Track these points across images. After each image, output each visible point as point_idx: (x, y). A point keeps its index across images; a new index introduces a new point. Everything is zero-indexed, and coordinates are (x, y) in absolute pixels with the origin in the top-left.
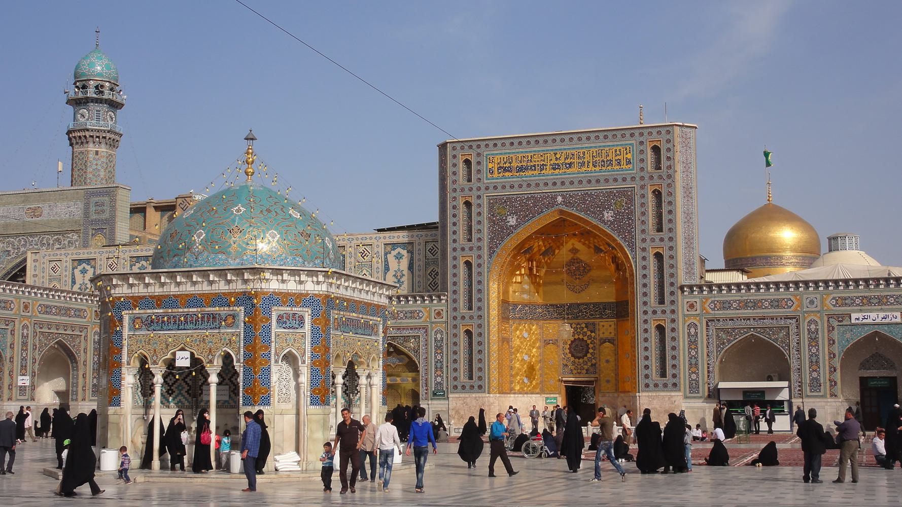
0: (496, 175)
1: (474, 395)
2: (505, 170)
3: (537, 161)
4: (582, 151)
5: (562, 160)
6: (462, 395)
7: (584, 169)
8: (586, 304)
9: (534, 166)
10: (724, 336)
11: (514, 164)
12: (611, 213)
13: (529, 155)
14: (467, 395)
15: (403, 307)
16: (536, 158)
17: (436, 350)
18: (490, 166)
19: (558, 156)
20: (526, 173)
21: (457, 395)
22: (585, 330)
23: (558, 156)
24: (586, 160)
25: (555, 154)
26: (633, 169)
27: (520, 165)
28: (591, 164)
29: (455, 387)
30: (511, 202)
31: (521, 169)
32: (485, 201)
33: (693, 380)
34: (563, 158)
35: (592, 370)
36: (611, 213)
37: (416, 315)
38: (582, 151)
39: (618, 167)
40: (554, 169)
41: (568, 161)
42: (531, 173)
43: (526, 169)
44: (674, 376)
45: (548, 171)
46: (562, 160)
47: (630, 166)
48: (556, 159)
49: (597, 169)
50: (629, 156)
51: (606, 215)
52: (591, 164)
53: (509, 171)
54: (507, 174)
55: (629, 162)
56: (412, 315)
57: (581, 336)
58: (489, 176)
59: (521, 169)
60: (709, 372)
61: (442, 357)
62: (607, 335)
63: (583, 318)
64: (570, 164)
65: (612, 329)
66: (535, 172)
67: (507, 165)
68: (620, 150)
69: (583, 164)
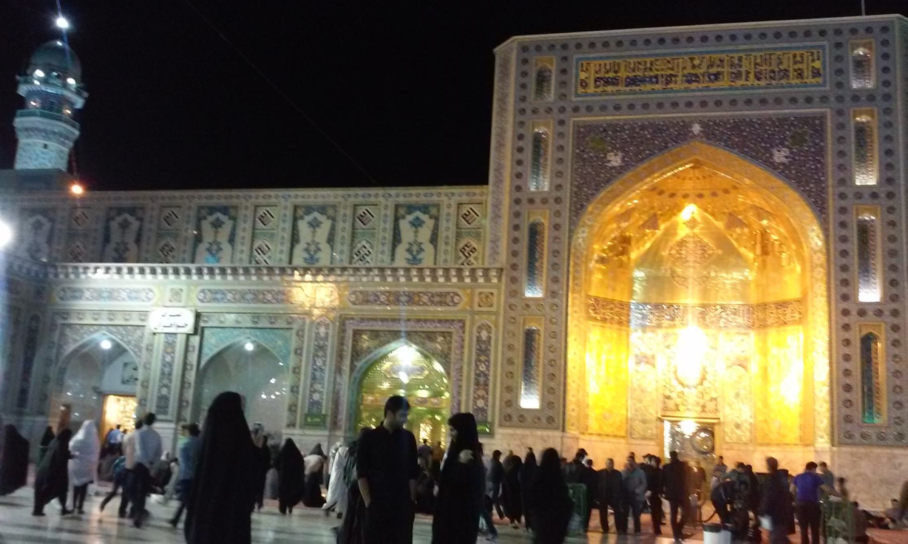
0: (591, 89)
1: (539, 433)
2: (607, 82)
3: (661, 68)
4: (736, 55)
6: (519, 432)
7: (739, 83)
9: (656, 77)
11: (623, 74)
12: (785, 152)
13: (648, 60)
14: (527, 432)
15: (429, 285)
16: (659, 65)
17: (478, 355)
18: (583, 75)
19: (696, 62)
20: (642, 88)
21: (510, 431)
23: (696, 62)
24: (743, 70)
25: (692, 59)
26: (824, 84)
27: (631, 75)
28: (752, 76)
29: (508, 417)
30: (615, 131)
31: (632, 81)
32: (570, 130)
34: (704, 66)
36: (785, 152)
37: (448, 299)
39: (798, 81)
40: (689, 82)
41: (714, 70)
42: (649, 87)
43: (643, 81)
45: (679, 85)
47: (820, 80)
48: (694, 67)
49: (763, 83)
50: (817, 64)
51: (776, 153)
52: (752, 76)
53: (614, 84)
54: (610, 88)
55: (816, 73)
56: (442, 299)
58: (581, 90)
59: (632, 81)
61: (488, 367)
64: (717, 76)
66: (657, 87)
67: (611, 75)
68: (802, 56)
69: (738, 75)
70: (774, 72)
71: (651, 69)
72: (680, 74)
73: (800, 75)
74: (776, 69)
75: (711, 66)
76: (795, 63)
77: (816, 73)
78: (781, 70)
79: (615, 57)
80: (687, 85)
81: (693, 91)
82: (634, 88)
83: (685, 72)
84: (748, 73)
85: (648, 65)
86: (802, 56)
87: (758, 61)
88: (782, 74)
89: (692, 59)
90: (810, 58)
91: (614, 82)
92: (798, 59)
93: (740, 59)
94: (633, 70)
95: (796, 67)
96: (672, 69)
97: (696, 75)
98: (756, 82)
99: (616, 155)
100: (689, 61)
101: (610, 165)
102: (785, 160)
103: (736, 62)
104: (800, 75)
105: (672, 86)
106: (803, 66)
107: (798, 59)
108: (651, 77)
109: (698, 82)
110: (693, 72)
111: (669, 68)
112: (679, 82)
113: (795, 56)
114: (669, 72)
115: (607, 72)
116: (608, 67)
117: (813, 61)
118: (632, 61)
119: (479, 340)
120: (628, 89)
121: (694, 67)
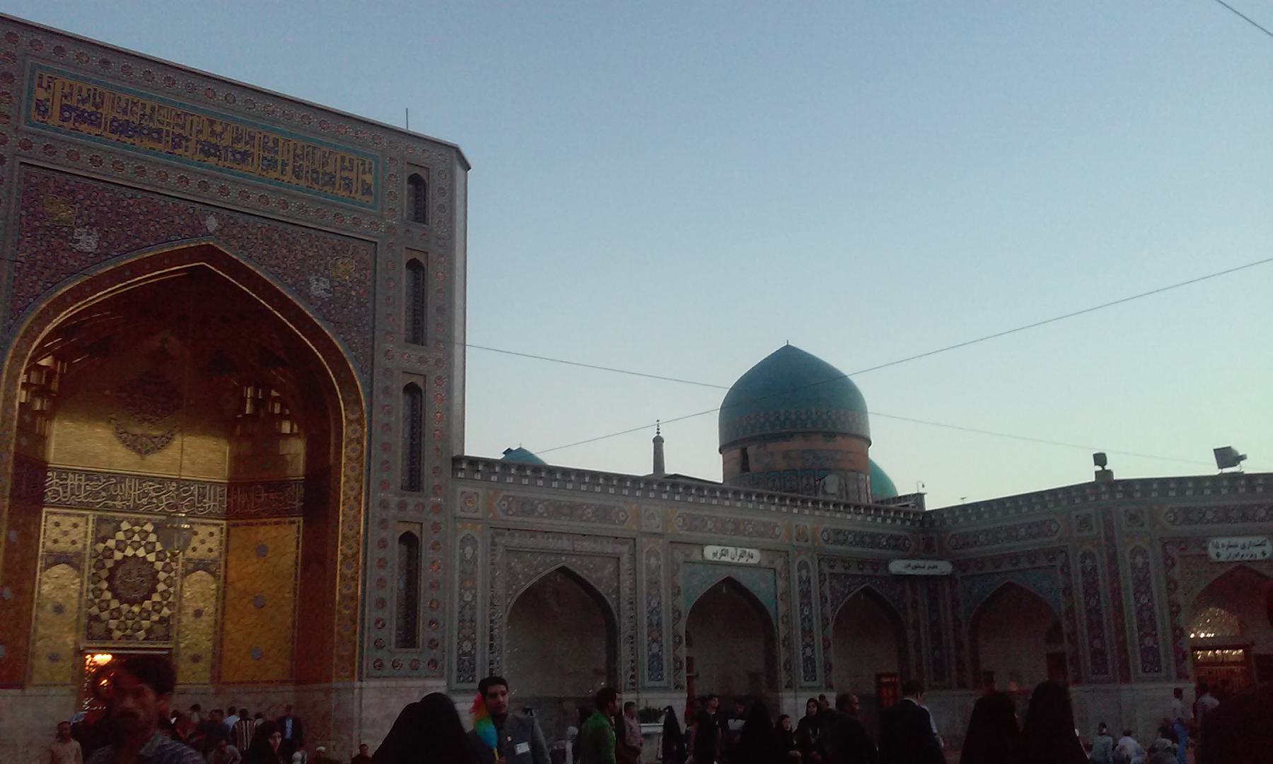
2: (82, 117)
5: (226, 141)
7: (274, 175)
8: (162, 481)
9: (159, 132)
10: (519, 567)
19: (218, 129)
22: (153, 538)
25: (212, 122)
28: (289, 169)
31: (122, 128)
33: (465, 654)
35: (160, 630)
38: (272, 136)
39: (342, 193)
40: (208, 154)
41: (240, 147)
42: (148, 144)
43: (137, 131)
44: (433, 644)
46: (226, 141)
48: (213, 133)
49: (303, 183)
50: (369, 178)
52: (289, 169)
53: (92, 123)
54: (84, 127)
57: (141, 553)
59: (122, 128)
60: (492, 638)
62: (202, 552)
63: (150, 512)
64: (245, 154)
65: (213, 543)
67: (89, 107)
68: (351, 161)
69: (272, 164)
70: (315, 171)
71: (151, 119)
72: (194, 138)
73: (348, 187)
74: (321, 170)
75: (236, 140)
76: (343, 169)
77: (367, 190)
78: (325, 174)
79: (96, 82)
80: (202, 156)
81: (210, 168)
82: (123, 138)
83: (202, 138)
84: (284, 164)
85: (148, 111)
86: (351, 161)
87: (299, 152)
88: (327, 178)
89: (212, 122)
90: (361, 168)
91: (92, 119)
92: (347, 164)
93: (276, 141)
94: (125, 113)
95: (345, 174)
96: (183, 128)
97: (216, 147)
98: (295, 180)
99: (89, 234)
100: (207, 123)
101: (77, 246)
102: (326, 295)
103: (271, 144)
104: (348, 187)
105: (180, 151)
106: (353, 175)
107: (347, 164)
108: (151, 131)
109: (219, 158)
110: (213, 140)
111: (178, 125)
112: (191, 150)
113: (343, 159)
114: (178, 131)
115: (84, 101)
116: (85, 94)
117: (364, 173)
118: (124, 97)
119: (1134, 567)
120: (115, 137)
121: (213, 133)
